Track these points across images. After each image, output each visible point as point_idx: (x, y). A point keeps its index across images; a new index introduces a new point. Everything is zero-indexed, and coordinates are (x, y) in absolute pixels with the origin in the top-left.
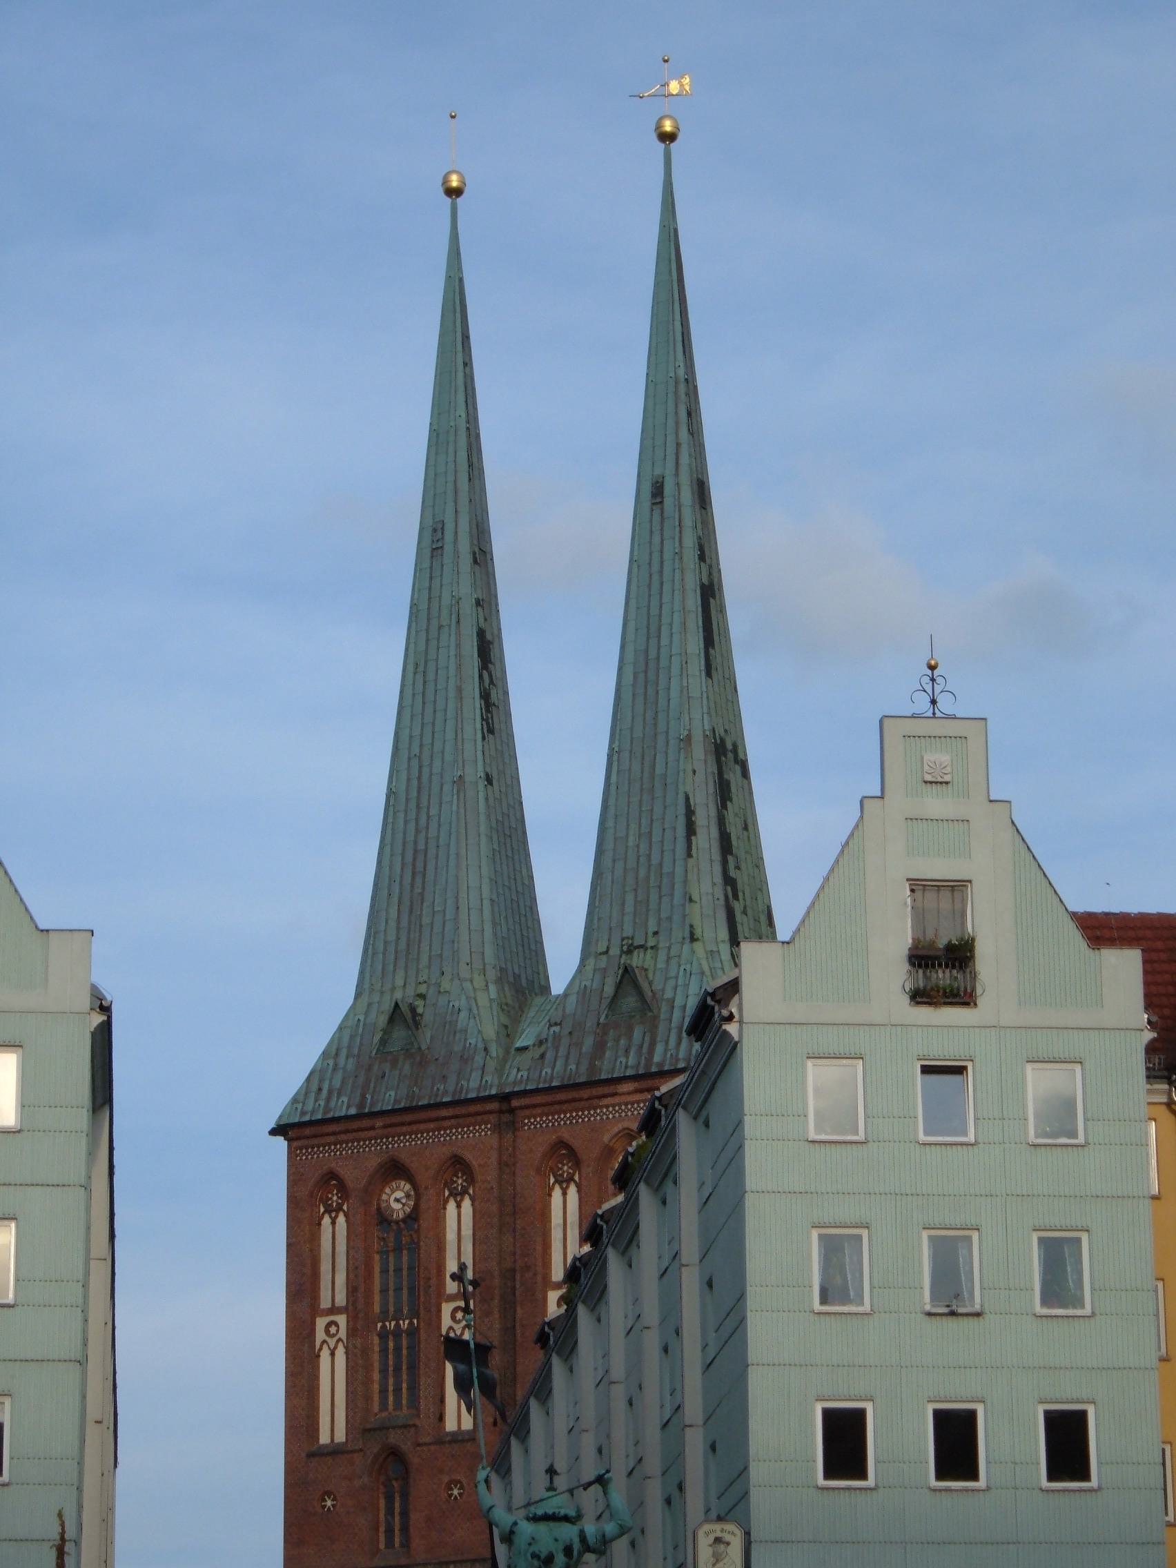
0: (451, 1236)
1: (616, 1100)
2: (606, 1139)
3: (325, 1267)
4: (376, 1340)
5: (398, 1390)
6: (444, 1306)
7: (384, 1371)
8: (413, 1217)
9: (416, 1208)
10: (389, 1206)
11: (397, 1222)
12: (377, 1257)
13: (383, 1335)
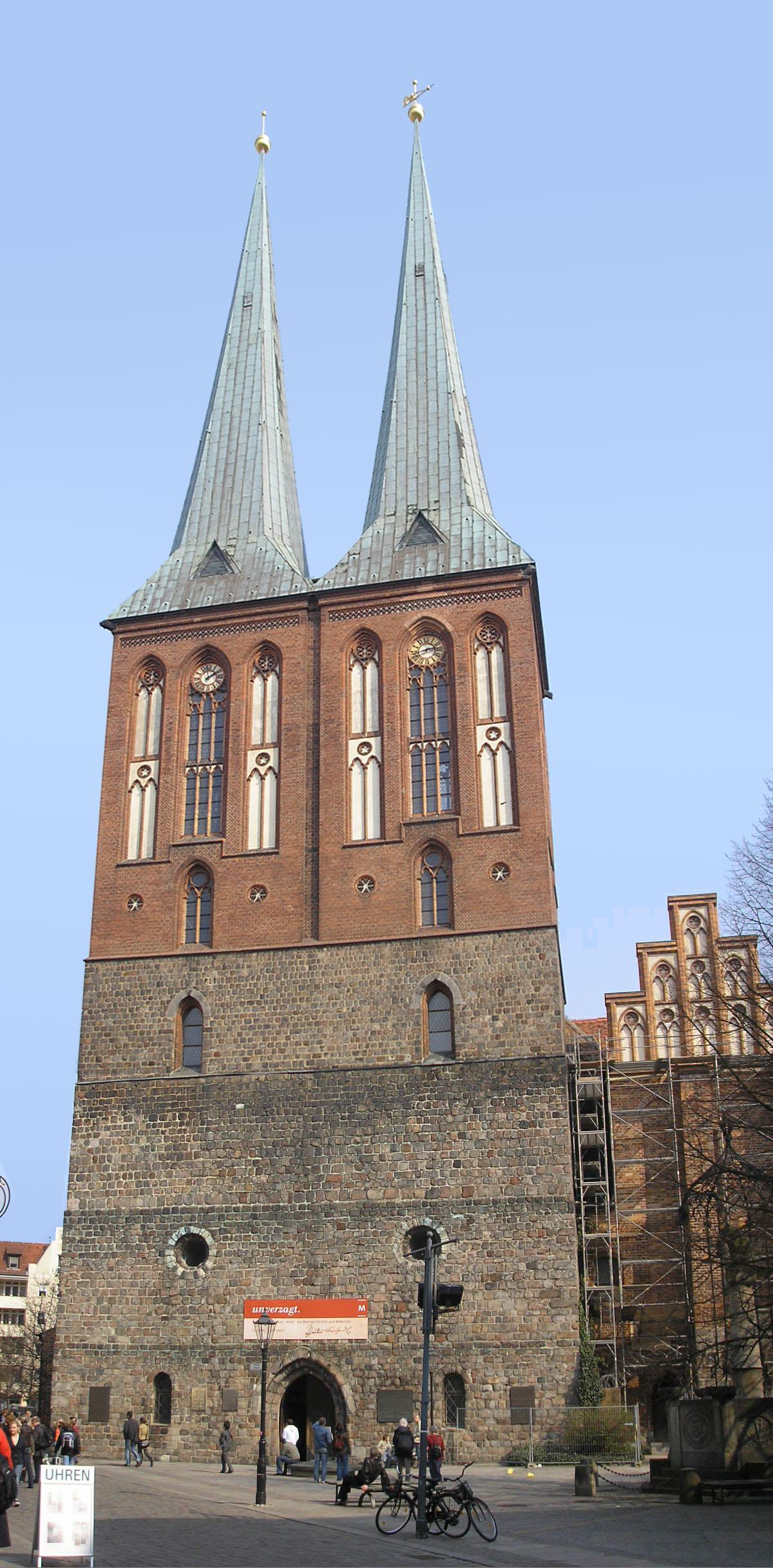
0: (257, 702)
1: (416, 597)
2: (406, 625)
3: (140, 726)
4: (185, 780)
5: (203, 819)
6: (249, 753)
7: (191, 805)
8: (224, 688)
9: (224, 683)
10: (200, 682)
11: (208, 694)
12: (188, 718)
13: (191, 778)
